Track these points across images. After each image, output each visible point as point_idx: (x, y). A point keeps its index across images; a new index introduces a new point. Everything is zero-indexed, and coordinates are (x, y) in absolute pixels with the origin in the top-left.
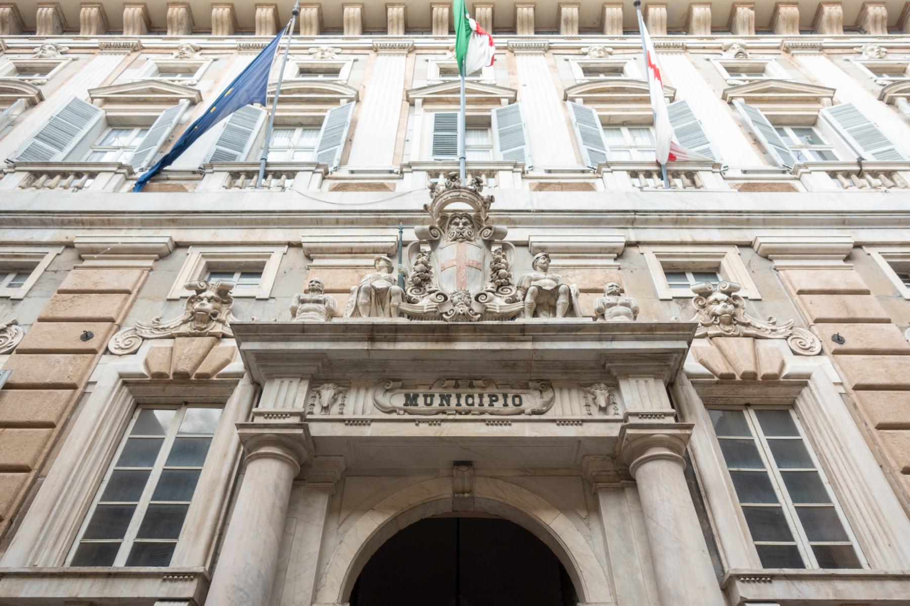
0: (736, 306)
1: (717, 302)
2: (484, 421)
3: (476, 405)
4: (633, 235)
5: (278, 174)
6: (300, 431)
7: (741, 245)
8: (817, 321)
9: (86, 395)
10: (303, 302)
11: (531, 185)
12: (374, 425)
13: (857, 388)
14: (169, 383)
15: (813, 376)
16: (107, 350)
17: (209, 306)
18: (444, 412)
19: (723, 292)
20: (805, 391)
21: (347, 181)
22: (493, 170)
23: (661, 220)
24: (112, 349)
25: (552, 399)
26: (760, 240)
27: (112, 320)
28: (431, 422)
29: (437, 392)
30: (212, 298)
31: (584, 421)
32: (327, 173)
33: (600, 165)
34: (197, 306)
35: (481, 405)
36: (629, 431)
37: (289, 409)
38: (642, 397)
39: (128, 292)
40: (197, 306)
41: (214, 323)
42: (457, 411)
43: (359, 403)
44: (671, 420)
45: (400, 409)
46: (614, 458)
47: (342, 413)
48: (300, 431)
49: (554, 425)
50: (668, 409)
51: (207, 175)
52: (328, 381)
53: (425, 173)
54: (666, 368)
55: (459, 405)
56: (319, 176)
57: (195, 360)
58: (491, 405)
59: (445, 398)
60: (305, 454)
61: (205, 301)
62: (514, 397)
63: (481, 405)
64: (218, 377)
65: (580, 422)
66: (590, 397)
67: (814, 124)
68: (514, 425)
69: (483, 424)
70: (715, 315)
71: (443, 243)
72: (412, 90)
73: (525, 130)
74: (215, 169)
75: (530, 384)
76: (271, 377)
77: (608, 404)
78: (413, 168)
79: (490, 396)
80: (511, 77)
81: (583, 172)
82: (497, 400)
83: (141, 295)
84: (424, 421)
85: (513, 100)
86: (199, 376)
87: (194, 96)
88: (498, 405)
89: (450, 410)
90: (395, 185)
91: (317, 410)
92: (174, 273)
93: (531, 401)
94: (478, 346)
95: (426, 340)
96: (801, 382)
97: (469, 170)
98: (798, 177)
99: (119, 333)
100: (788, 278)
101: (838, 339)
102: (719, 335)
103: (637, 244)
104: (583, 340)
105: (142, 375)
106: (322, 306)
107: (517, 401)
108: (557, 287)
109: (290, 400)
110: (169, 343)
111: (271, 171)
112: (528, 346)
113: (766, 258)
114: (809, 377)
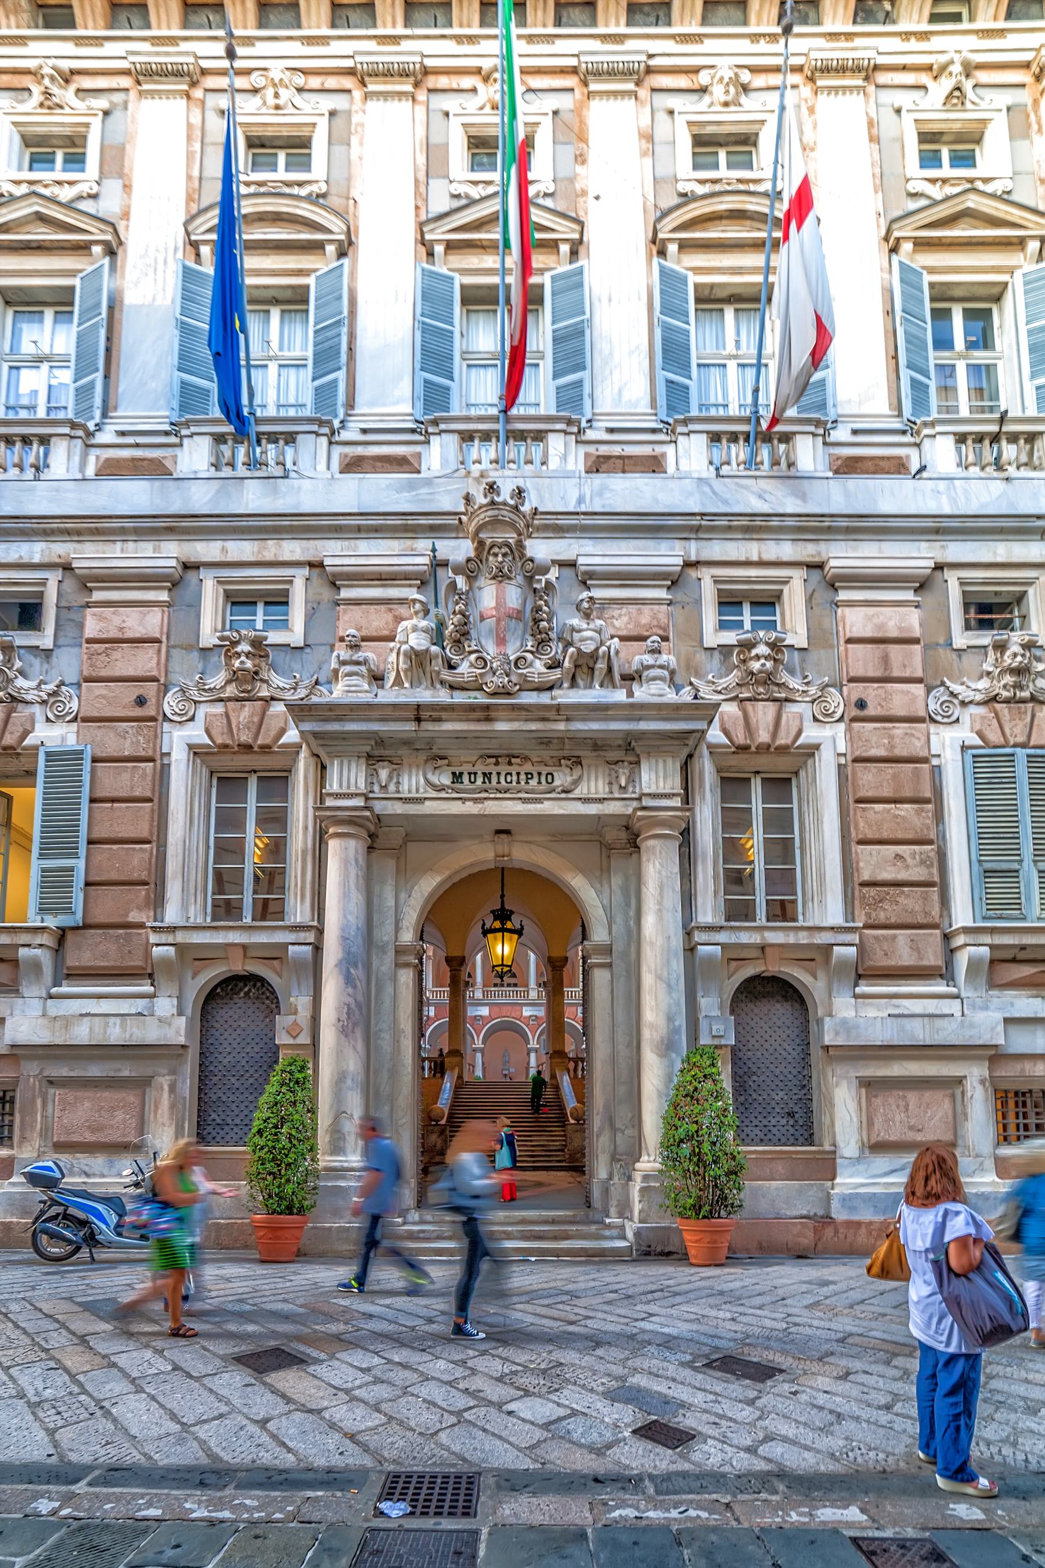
0: (775, 660)
1: (758, 657)
4: (694, 550)
5: (273, 437)
6: (368, 814)
7: (810, 566)
11: (587, 455)
12: (427, 803)
17: (249, 664)
19: (767, 644)
21: (360, 450)
22: (541, 431)
23: (730, 527)
25: (580, 778)
26: (833, 563)
28: (475, 800)
29: (480, 768)
32: (333, 433)
33: (676, 421)
34: (237, 664)
35: (518, 782)
37: (353, 790)
38: (656, 778)
40: (237, 664)
44: (677, 802)
46: (627, 828)
47: (398, 792)
48: (368, 814)
51: (186, 441)
52: (381, 759)
53: (456, 436)
54: (685, 748)
56: (324, 441)
58: (527, 783)
59: (487, 776)
60: (372, 828)
61: (243, 658)
63: (518, 782)
65: (601, 800)
66: (614, 775)
67: (998, 299)
68: (547, 804)
70: (752, 673)
72: (429, 221)
73: (587, 332)
74: (193, 429)
76: (332, 756)
77: (627, 783)
78: (442, 426)
80: (579, 169)
81: (654, 431)
84: (469, 799)
85: (574, 254)
87: (108, 237)
88: (533, 782)
91: (376, 788)
93: (562, 778)
97: (513, 431)
98: (918, 441)
100: (844, 618)
102: (749, 699)
103: (696, 564)
106: (363, 668)
109: (353, 781)
111: (264, 433)
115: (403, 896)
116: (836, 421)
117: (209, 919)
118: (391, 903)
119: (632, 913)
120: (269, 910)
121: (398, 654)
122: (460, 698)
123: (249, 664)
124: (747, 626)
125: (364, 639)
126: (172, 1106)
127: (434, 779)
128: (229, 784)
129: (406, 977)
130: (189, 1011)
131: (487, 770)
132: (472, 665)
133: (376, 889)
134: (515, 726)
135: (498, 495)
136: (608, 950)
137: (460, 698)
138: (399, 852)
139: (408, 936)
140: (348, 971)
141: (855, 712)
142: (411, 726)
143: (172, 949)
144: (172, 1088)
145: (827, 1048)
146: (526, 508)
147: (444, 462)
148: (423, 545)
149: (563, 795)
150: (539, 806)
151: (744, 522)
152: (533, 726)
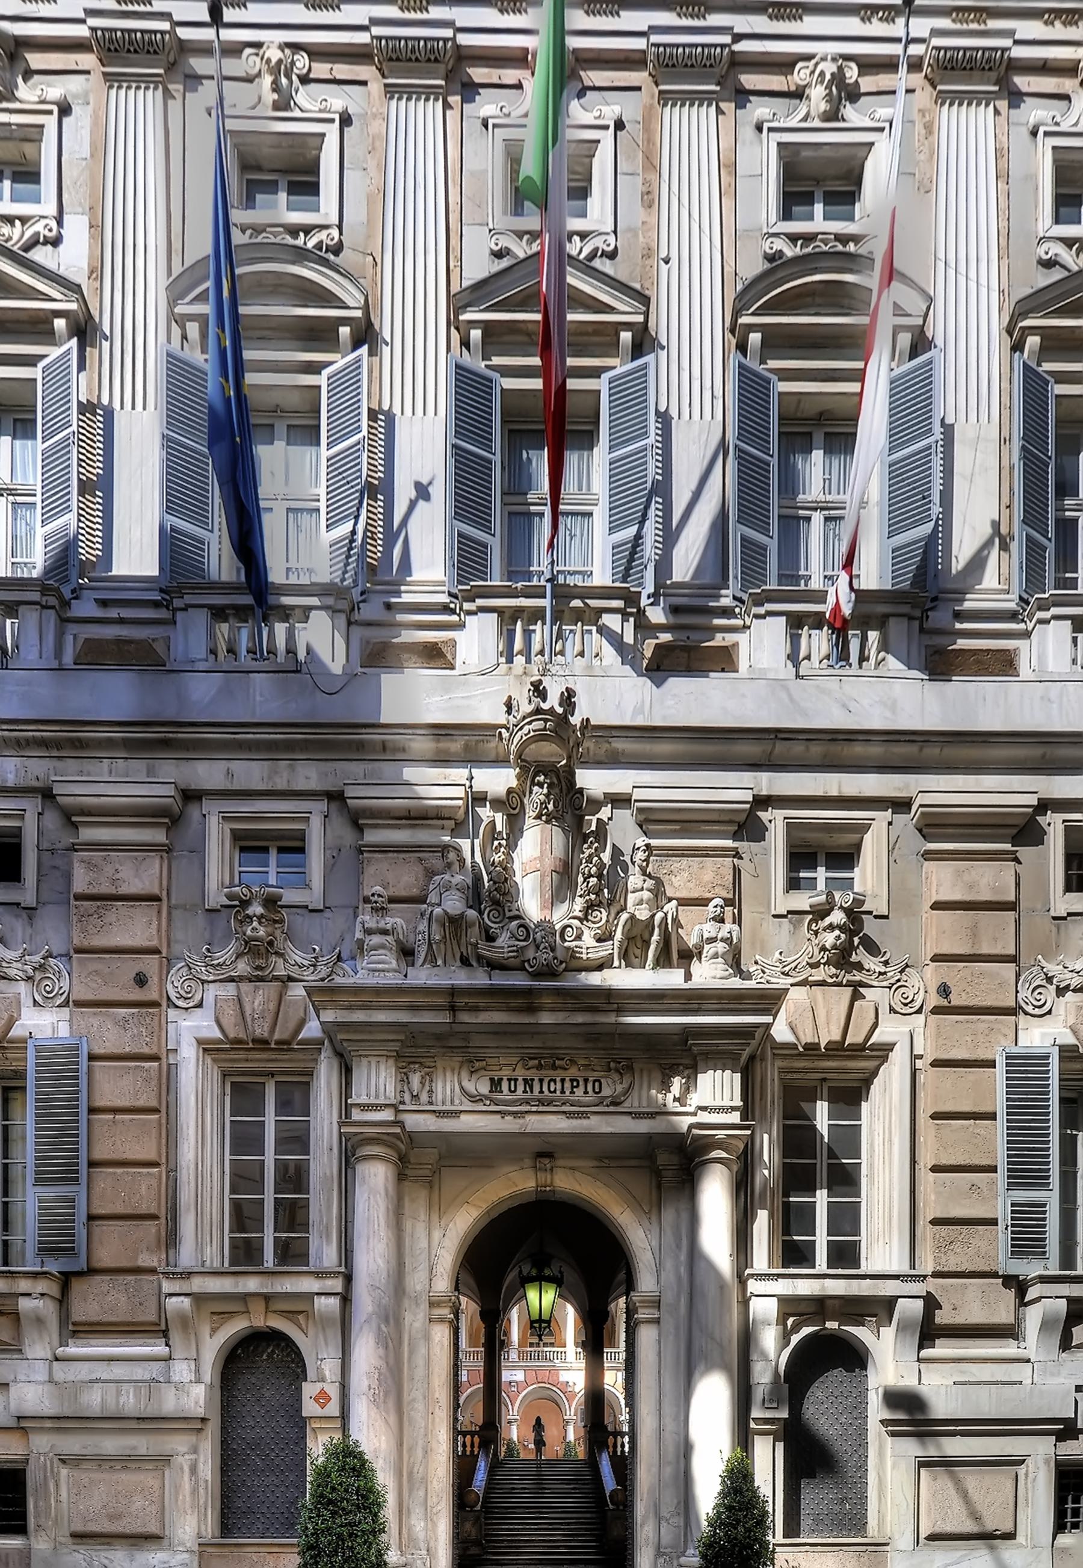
3: (558, 1092)
9: (173, 1067)
12: (463, 1117)
24: (173, 995)
27: (156, 951)
29: (520, 1073)
35: (563, 1092)
39: (157, 899)
41: (274, 958)
42: (539, 1100)
43: (448, 1087)
44: (735, 1118)
45: (487, 1098)
50: (738, 1102)
55: (541, 1092)
57: (269, 1019)
58: (572, 1092)
62: (594, 1082)
63: (563, 1092)
69: (563, 1117)
75: (612, 1065)
79: (572, 1081)
83: (173, 902)
88: (579, 1091)
89: (533, 1100)
90: (453, 643)
92: (199, 851)
99: (172, 972)
105: (220, 1042)
107: (597, 1084)
110: (230, 989)
115: (437, 1235)
116: (935, 599)
117: (226, 1264)
118: (424, 1244)
119: (683, 1257)
120: (292, 1254)
121: (430, 920)
122: (501, 980)
124: (821, 885)
125: (392, 900)
126: (194, 1491)
127: (470, 1086)
128: (243, 1093)
129: (441, 1335)
130: (207, 1377)
131: (529, 1074)
132: (513, 936)
133: (408, 1225)
134: (559, 1018)
135: (544, 700)
136: (657, 1304)
137: (501, 980)
138: (431, 1183)
139: (443, 1285)
140: (379, 1328)
142: (444, 1018)
143: (186, 1302)
144: (194, 1470)
146: (575, 720)
147: (483, 652)
148: (459, 774)
149: (612, 1109)
150: (585, 1122)
152: (580, 1018)
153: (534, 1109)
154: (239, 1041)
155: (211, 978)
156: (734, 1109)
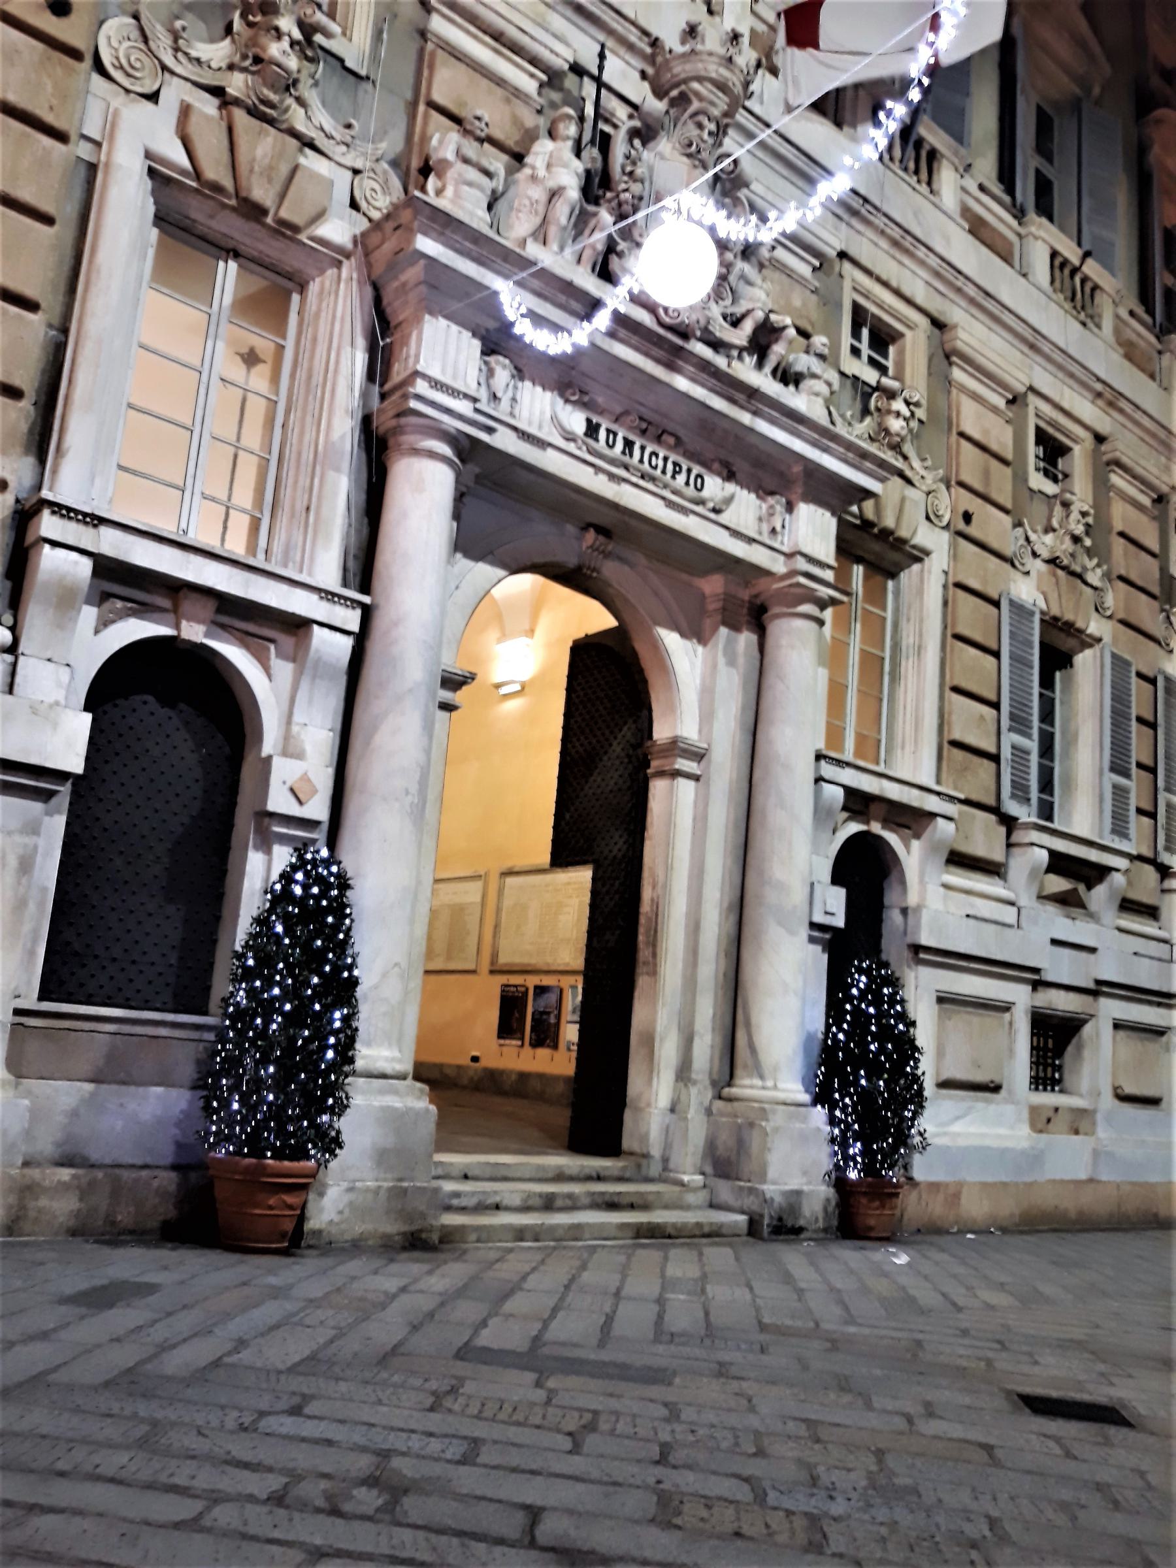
2: (663, 498)
8: (961, 484)
10: (466, 161)
12: (550, 451)
13: (959, 585)
14: (225, 206)
15: (933, 556)
16: (99, 67)
17: (293, 63)
18: (626, 467)
20: (916, 567)
28: (612, 477)
30: (298, 43)
31: (754, 540)
35: (664, 472)
36: (802, 580)
47: (512, 415)
49: (726, 533)
55: (641, 461)
58: (673, 477)
59: (629, 444)
62: (699, 476)
63: (664, 472)
64: (312, 239)
65: (751, 540)
68: (692, 517)
70: (887, 431)
71: (665, 145)
79: (675, 464)
82: (680, 472)
86: (283, 223)
88: (681, 479)
93: (714, 487)
94: (699, 392)
95: (647, 354)
96: (919, 556)
101: (967, 517)
104: (798, 435)
105: (183, 172)
108: (784, 328)
112: (746, 418)
113: (947, 357)
114: (927, 553)
123: (293, 63)
141: (961, 525)
145: (917, 949)
149: (712, 516)
151: (896, 233)
153: (634, 479)
154: (217, 188)
155: (178, 69)
156: (830, 567)
